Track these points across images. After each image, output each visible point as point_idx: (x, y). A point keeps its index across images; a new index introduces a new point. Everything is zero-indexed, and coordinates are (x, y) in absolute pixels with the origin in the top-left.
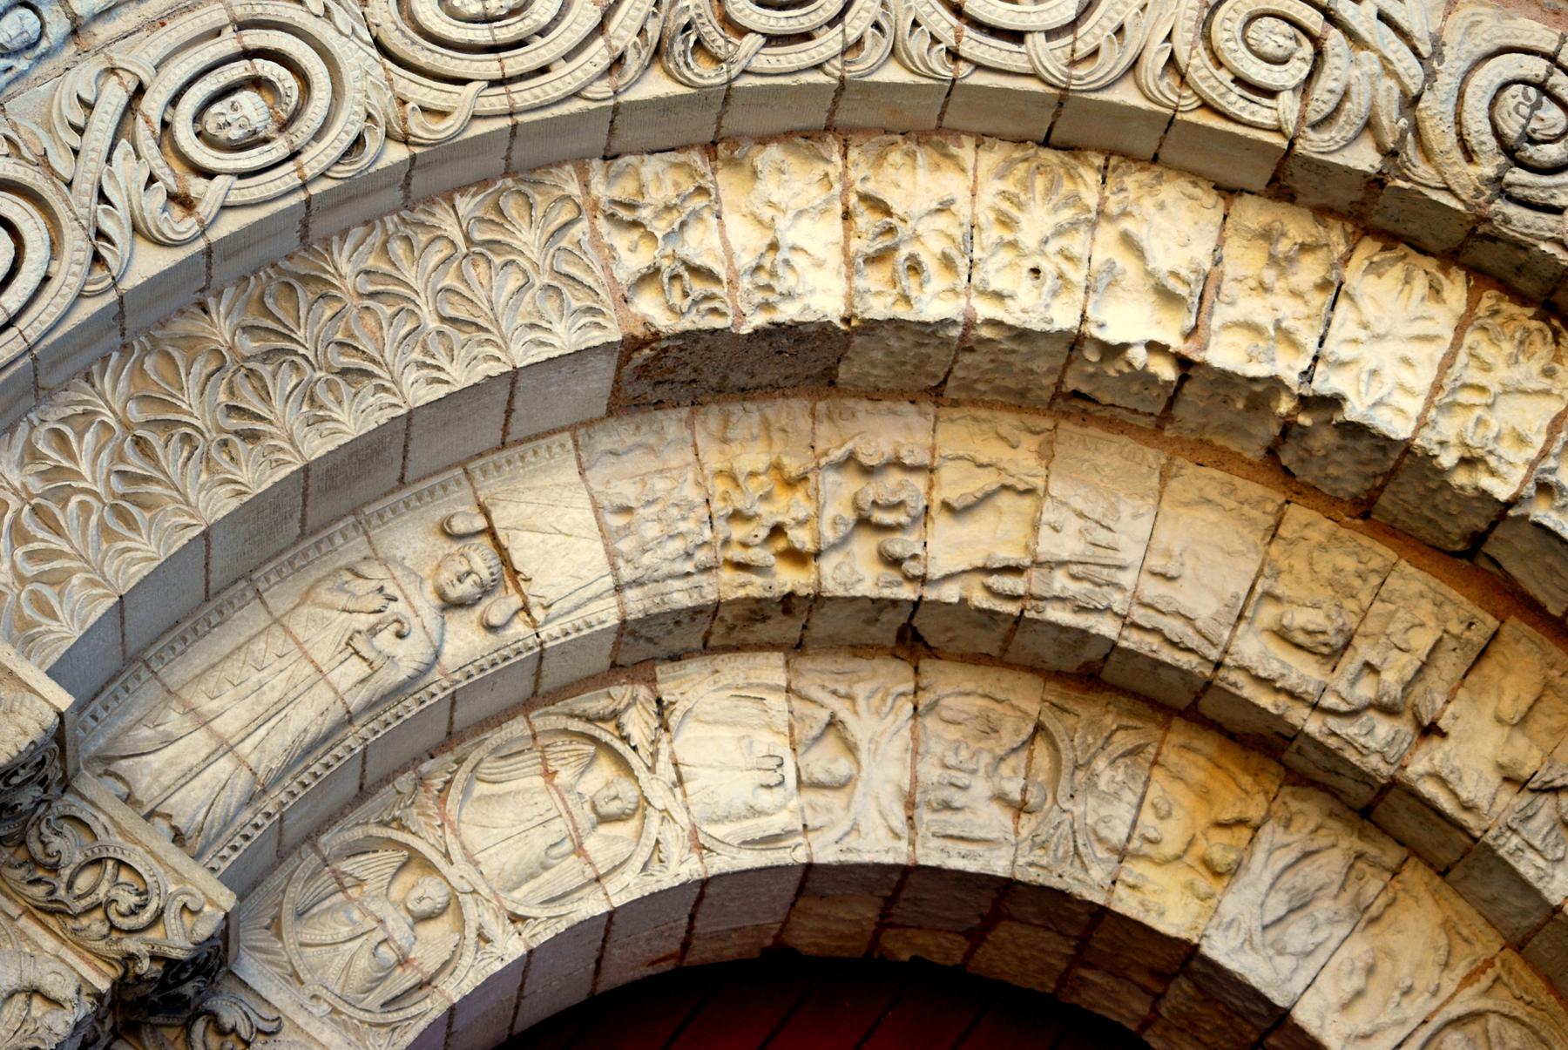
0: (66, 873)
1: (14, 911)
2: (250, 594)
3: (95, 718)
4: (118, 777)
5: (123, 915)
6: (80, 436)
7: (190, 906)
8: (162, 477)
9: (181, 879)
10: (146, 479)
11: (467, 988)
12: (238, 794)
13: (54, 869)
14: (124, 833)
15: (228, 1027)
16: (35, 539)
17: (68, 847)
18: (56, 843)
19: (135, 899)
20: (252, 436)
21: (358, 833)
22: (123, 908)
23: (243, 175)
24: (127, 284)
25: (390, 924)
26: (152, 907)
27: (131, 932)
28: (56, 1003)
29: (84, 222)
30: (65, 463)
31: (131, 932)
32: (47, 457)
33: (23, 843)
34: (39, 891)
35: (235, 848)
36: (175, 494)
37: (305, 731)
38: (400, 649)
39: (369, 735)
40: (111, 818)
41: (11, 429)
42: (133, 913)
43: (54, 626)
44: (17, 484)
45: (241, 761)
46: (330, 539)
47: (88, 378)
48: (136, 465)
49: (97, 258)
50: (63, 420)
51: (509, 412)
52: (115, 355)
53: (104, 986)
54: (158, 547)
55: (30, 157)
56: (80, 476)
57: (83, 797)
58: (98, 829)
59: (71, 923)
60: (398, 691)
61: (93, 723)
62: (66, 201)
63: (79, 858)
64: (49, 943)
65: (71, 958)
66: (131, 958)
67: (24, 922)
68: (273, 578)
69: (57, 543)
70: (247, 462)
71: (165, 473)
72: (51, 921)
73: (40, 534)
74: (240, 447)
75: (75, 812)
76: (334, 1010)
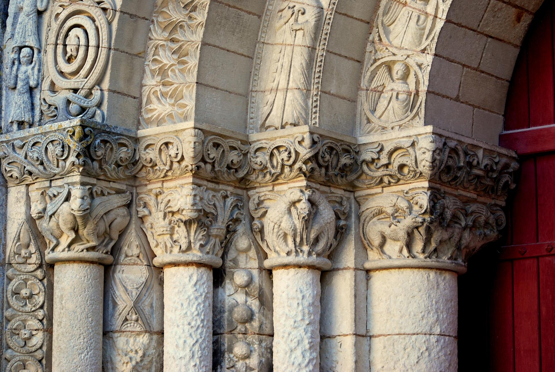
0: (269, 165)
1: (270, 188)
2: (261, 46)
3: (252, 118)
4: (269, 127)
5: (288, 160)
6: (159, 55)
7: (300, 139)
8: (183, 42)
9: (292, 135)
10: (180, 47)
11: (427, 83)
12: (299, 99)
13: (266, 168)
14: (271, 140)
15: (370, 159)
16: (168, 92)
17: (262, 158)
18: (258, 160)
19: (287, 153)
20: (194, 9)
21: (369, 74)
22: (286, 159)
24: (118, 7)
25: (395, 88)
26: (292, 151)
27: (294, 163)
28: (299, 201)
29: (92, 5)
30: (160, 65)
31: (294, 163)
32: (156, 69)
33: (254, 169)
34: (268, 177)
35: (315, 113)
36: (189, 43)
37: (301, 64)
38: (307, 16)
39: (323, 47)
40: (265, 139)
41: (144, 72)
42: (290, 157)
43: (188, 108)
44: (155, 83)
45: (291, 89)
46: (268, 9)
47: (150, 39)
48: (175, 46)
49: (105, 10)
50: (153, 56)
52: (152, 26)
53: (304, 183)
54: (194, 61)
55: (67, 4)
56: (166, 65)
57: (255, 142)
58: (264, 145)
59: (283, 176)
60: (318, 27)
61: (251, 121)
62: (83, 4)
63: (267, 158)
64: (285, 187)
65: (292, 185)
66: (300, 169)
67: (276, 188)
68: (263, 35)
69: (173, 87)
70: (197, 16)
71: (183, 41)
72: (280, 181)
73: (168, 89)
74: (193, 14)
75: (256, 147)
76: (400, 126)
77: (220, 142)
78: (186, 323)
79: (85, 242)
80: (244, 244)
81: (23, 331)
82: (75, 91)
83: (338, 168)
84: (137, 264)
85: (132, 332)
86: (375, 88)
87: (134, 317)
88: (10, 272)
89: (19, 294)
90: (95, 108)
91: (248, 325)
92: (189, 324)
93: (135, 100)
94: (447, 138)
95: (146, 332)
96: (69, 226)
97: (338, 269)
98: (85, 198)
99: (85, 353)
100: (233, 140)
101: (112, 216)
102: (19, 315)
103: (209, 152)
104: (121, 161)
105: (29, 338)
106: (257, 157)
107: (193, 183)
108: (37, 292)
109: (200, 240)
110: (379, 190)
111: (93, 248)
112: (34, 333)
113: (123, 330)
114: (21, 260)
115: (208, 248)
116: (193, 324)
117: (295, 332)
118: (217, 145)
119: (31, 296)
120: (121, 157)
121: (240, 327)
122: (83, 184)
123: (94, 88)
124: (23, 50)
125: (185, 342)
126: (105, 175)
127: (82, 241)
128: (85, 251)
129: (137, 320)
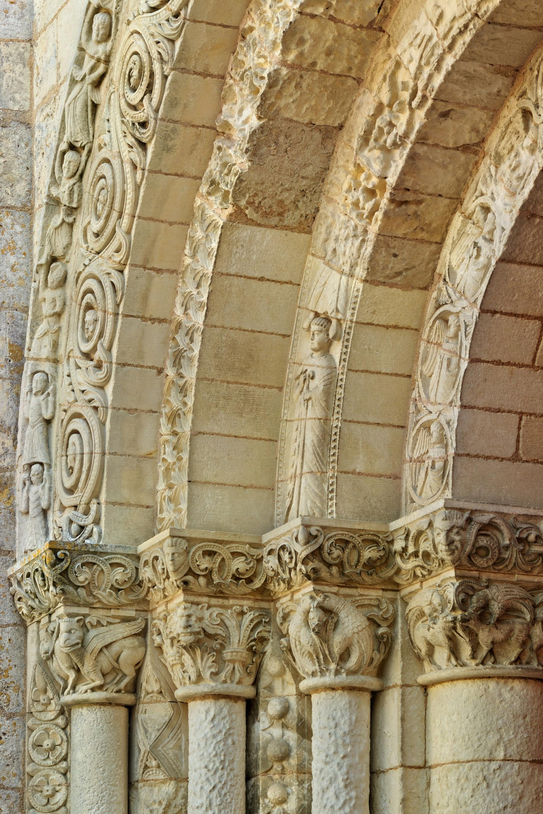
3: (278, 515)
12: (312, 484)
13: (278, 574)
21: (411, 441)
23: (101, 335)
26: (293, 551)
35: (331, 499)
37: (312, 441)
39: (337, 416)
51: (262, 279)
77: (214, 550)
78: (203, 766)
79: (90, 681)
80: (275, 667)
81: (46, 788)
83: (361, 564)
84: (160, 702)
85: (156, 780)
86: (418, 458)
87: (154, 763)
88: (30, 723)
89: (42, 746)
90: (92, 526)
91: (284, 763)
92: (206, 767)
93: (148, 509)
94: (473, 512)
95: (171, 779)
96: (66, 665)
97: (389, 688)
98: (73, 631)
99: (96, 808)
100: (237, 545)
101: (115, 648)
102: (39, 771)
103: (198, 563)
104: (118, 584)
105: (53, 795)
107: (186, 601)
108: (59, 742)
109: (210, 667)
110: (417, 586)
111: (100, 688)
112: (58, 788)
113: (145, 779)
114: (40, 708)
115: (222, 676)
116: (210, 767)
117: (327, 768)
118: (211, 554)
119: (53, 748)
120: (117, 580)
121: (277, 767)
122: (71, 615)
125: (202, 788)
126: (100, 601)
127: (87, 680)
128: (89, 691)
129: (159, 767)
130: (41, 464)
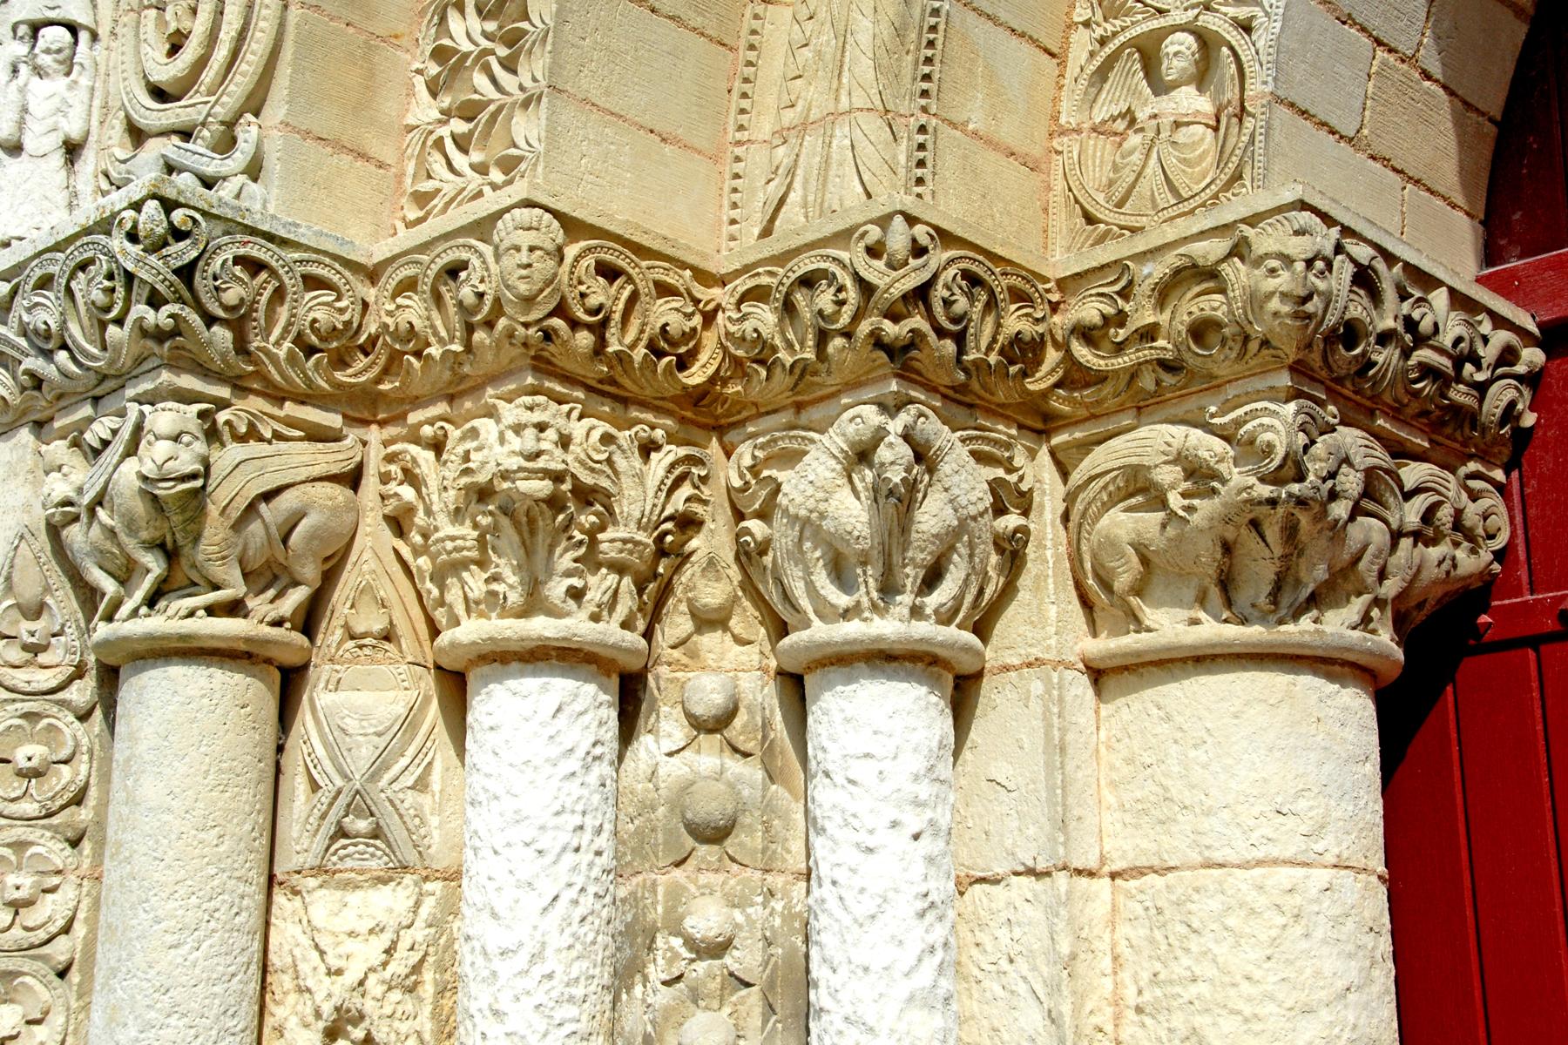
27: (857, 317)
77: (622, 263)
80: (713, 596)
82: (186, 135)
83: (997, 347)
86: (1104, 122)
89: (8, 762)
90: (243, 178)
93: (381, 171)
98: (186, 438)
99: (191, 943)
100: (666, 265)
101: (287, 501)
103: (583, 288)
106: (744, 318)
113: (330, 866)
118: (609, 272)
120: (315, 321)
123: (242, 121)
124: (43, 31)
128: (201, 613)
130: (73, 29)
